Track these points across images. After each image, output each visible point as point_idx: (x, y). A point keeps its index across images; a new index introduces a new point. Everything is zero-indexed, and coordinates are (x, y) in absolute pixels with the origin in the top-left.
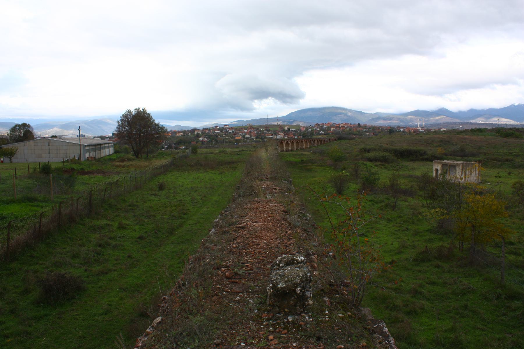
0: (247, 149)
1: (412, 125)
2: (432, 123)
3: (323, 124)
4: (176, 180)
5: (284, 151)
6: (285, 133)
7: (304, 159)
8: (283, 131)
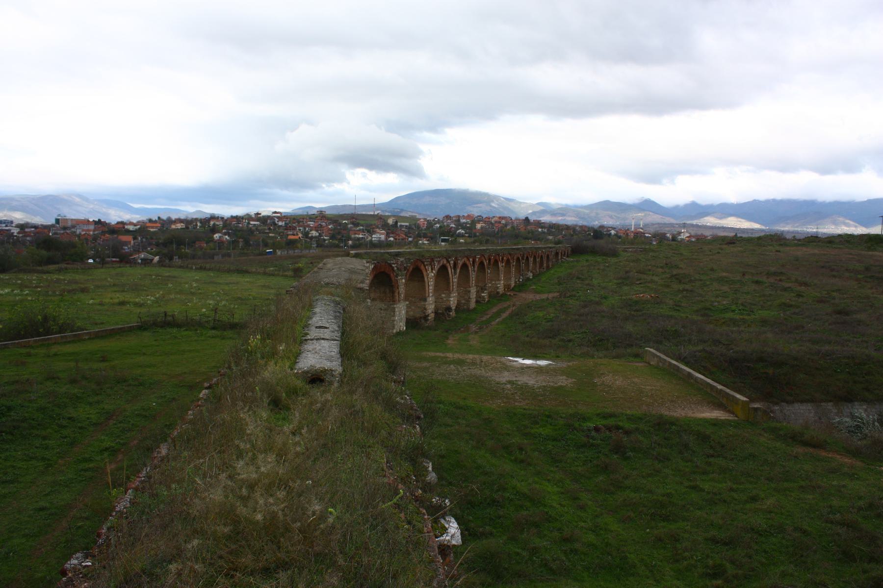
6: (390, 231)
8: (385, 226)
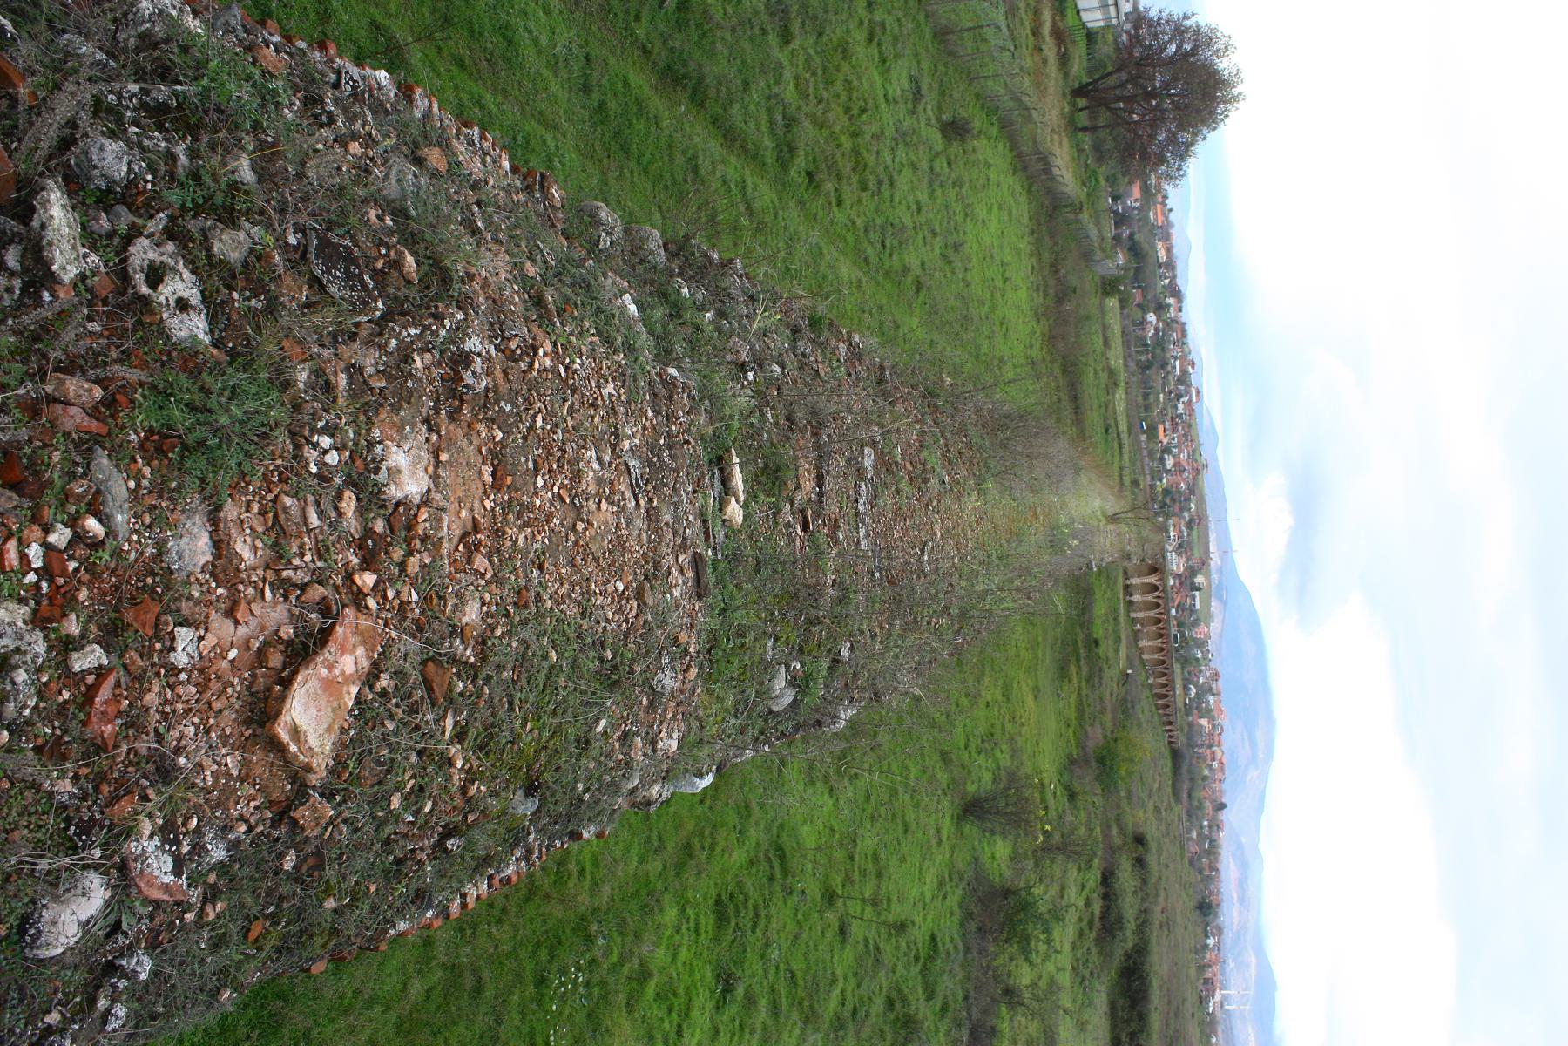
0: (1126, 457)
1: (1228, 970)
2: (1235, 1032)
3: (1219, 694)
4: (993, 201)
5: (1127, 578)
7: (1101, 650)
8: (1192, 572)
